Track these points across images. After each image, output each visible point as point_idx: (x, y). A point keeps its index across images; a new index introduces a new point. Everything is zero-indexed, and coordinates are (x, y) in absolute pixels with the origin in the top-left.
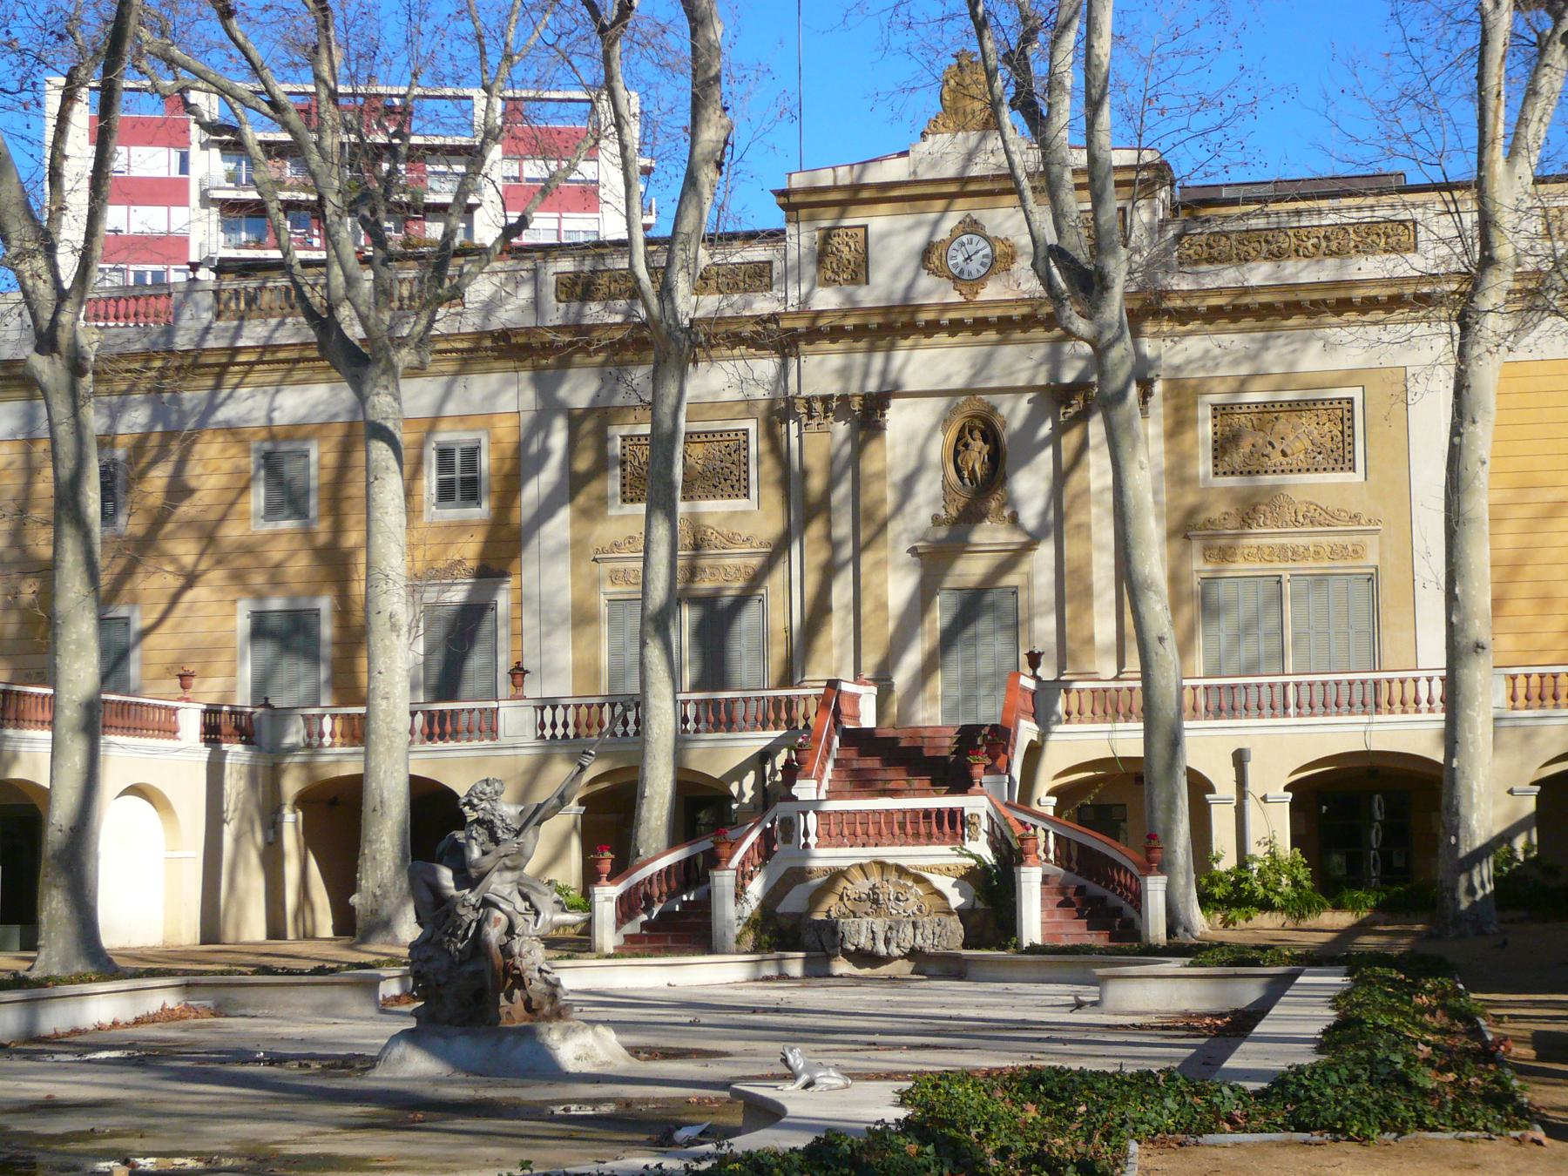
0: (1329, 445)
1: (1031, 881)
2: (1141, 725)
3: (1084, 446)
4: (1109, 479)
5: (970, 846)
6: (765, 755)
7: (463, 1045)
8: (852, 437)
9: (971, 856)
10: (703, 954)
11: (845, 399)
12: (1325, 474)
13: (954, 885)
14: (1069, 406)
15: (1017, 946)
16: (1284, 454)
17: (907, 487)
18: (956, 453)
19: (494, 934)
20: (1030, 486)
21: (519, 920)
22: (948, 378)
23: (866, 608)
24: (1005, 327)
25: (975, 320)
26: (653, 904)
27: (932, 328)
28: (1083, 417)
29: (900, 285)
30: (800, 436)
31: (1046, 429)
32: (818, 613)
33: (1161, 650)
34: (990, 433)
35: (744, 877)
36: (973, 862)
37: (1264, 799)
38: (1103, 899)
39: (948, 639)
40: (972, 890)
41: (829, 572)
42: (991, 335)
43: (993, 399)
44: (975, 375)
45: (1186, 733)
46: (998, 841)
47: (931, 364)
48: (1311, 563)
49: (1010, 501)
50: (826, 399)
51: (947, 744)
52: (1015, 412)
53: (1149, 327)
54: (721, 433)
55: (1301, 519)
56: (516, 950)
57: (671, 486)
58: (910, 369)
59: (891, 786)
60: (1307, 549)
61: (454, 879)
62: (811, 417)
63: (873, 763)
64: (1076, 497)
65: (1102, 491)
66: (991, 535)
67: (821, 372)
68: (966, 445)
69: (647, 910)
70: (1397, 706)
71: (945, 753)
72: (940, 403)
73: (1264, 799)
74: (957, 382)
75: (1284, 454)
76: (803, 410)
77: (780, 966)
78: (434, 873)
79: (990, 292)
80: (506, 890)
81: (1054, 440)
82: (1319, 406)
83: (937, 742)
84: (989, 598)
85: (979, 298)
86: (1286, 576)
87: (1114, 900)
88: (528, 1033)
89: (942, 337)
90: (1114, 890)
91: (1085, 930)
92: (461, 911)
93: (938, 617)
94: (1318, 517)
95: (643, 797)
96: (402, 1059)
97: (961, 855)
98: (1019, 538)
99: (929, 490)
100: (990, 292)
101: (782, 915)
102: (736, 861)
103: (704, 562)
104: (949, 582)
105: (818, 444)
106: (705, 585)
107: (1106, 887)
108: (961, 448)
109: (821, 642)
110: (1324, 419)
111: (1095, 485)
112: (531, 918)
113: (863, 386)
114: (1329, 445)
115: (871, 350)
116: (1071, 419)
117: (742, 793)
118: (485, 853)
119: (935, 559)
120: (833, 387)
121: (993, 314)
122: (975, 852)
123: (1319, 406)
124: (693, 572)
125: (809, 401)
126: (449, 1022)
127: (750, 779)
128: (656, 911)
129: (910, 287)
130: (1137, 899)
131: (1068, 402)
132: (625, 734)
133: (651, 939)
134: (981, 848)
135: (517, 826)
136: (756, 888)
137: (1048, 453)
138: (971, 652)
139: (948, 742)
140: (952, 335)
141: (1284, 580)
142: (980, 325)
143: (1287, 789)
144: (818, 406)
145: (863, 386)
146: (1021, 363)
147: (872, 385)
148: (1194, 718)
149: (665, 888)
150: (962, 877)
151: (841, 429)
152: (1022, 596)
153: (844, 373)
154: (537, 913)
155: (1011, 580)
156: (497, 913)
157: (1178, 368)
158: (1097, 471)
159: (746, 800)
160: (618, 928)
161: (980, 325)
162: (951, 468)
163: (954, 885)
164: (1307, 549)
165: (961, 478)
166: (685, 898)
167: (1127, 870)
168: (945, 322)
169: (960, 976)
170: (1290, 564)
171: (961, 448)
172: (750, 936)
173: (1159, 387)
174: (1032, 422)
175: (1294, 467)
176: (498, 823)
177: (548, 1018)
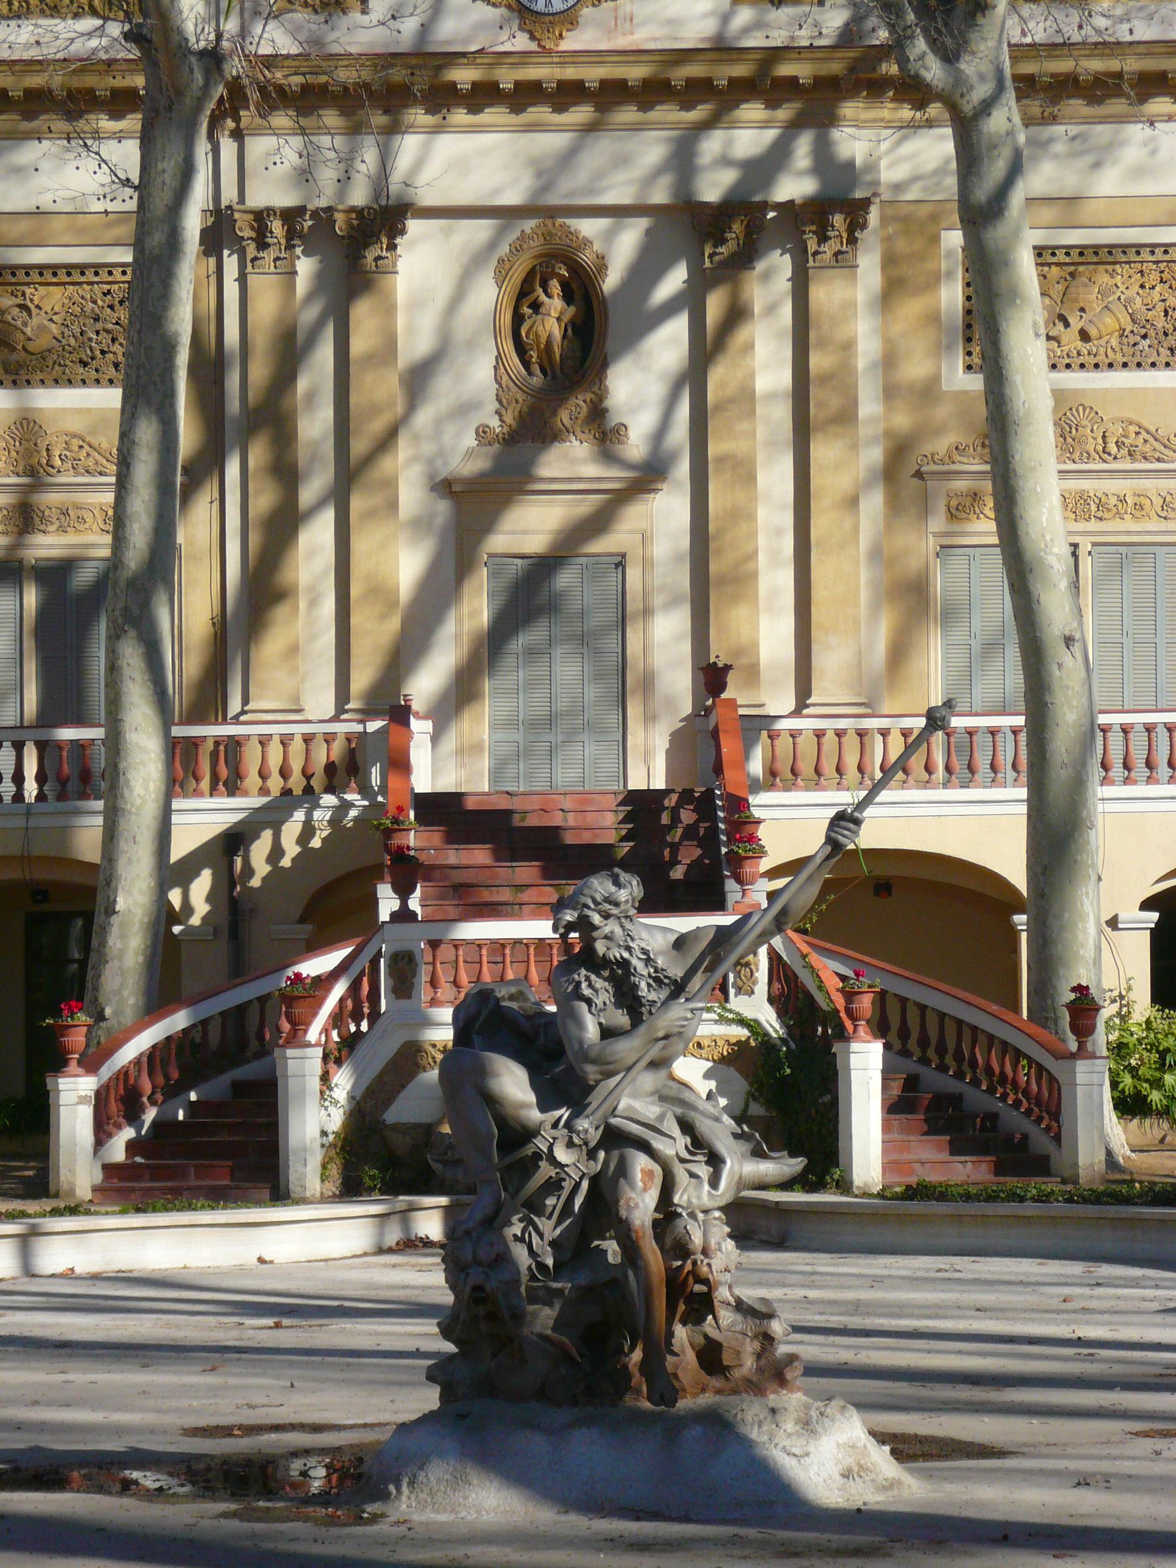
0: (1160, 323)
1: (866, 1064)
2: (1023, 793)
3: (736, 315)
4: (784, 378)
5: (738, 1003)
6: (233, 841)
7: (589, 1450)
8: (320, 281)
9: (742, 1022)
10: (259, 1203)
11: (324, 217)
12: (1153, 373)
13: (707, 1075)
14: (722, 241)
15: (844, 1185)
16: (1084, 336)
17: (418, 380)
18: (518, 319)
19: (641, 1204)
20: (639, 385)
21: (680, 1172)
22: (497, 191)
23: (355, 590)
24: (608, 97)
25: (562, 84)
26: (142, 1109)
27: (483, 95)
28: (745, 258)
29: (409, 26)
30: (242, 280)
31: (675, 280)
32: (260, 593)
33: (1067, 658)
34: (581, 287)
35: (333, 1058)
36: (742, 1033)
37: (1113, 923)
38: (956, 1100)
39: (491, 648)
40: (741, 1085)
41: (282, 527)
42: (581, 113)
43: (588, 227)
44: (545, 188)
45: (1100, 807)
46: (790, 994)
47: (462, 162)
48: (1129, 524)
49: (598, 414)
50: (290, 216)
51: (606, 826)
52: (618, 249)
53: (849, 109)
54: (97, 268)
55: (1113, 448)
56: (697, 1239)
57: (170, 348)
58: (426, 175)
59: (487, 896)
60: (1123, 500)
61: (536, 1084)
62: (262, 245)
63: (480, 855)
64: (718, 407)
65: (772, 396)
66: (570, 460)
67: (270, 166)
68: (536, 306)
69: (133, 1117)
70: (1117, 771)
71: (610, 838)
72: (479, 231)
73: (1113, 923)
74: (512, 197)
75: (1084, 336)
76: (247, 233)
77: (406, 1224)
78: (482, 1073)
79: (572, 42)
80: (650, 1110)
81: (691, 300)
82: (1145, 255)
83: (591, 819)
84: (565, 579)
85: (564, 46)
86: (1085, 546)
87: (977, 1099)
88: (718, 1424)
89: (493, 115)
90: (976, 1083)
91: (944, 1156)
92: (562, 1155)
93: (476, 608)
94: (1139, 445)
95: (111, 911)
96: (458, 1481)
97: (722, 1020)
98: (615, 476)
99: (479, 378)
100: (572, 42)
101: (395, 1127)
102: (314, 1033)
103: (50, 499)
104: (499, 542)
105: (228, 301)
106: (47, 545)
107: (959, 1075)
108: (526, 310)
109: (271, 646)
110: (1154, 277)
111: (762, 384)
112: (704, 1171)
113: (342, 194)
114: (1160, 323)
115: (355, 130)
116: (724, 264)
117: (188, 909)
118: (607, 1033)
119: (472, 504)
120: (285, 199)
121: (592, 74)
122: (749, 1014)
123: (1145, 255)
124: (26, 517)
125: (261, 217)
126: (544, 1394)
127: (202, 884)
128: (150, 1115)
129: (425, 29)
130: (1050, 1106)
131: (718, 235)
132: (19, 797)
133: (156, 1173)
134: (759, 1007)
135: (677, 972)
136: (343, 1081)
137: (677, 328)
138: (541, 669)
139: (610, 819)
140: (517, 109)
141: (1082, 553)
142: (567, 94)
143: (1146, 905)
144: (277, 227)
145: (342, 194)
146: (630, 164)
147: (359, 196)
148: (1105, 781)
149: (160, 1080)
150: (723, 1060)
151: (305, 267)
152: (633, 576)
153: (305, 175)
154: (715, 1160)
155: (598, 546)
156: (640, 1162)
157: (897, 187)
158: (764, 361)
159: (195, 920)
160: (96, 1152)
161: (567, 94)
162: (509, 347)
163: (707, 1075)
164: (1123, 500)
165: (526, 364)
166: (193, 1096)
167: (1018, 1054)
168: (506, 85)
169: (779, 1244)
170: (1093, 525)
171: (526, 310)
172: (334, 1170)
173: (874, 216)
174: (647, 269)
175: (1100, 358)
176: (637, 964)
177: (755, 1387)
